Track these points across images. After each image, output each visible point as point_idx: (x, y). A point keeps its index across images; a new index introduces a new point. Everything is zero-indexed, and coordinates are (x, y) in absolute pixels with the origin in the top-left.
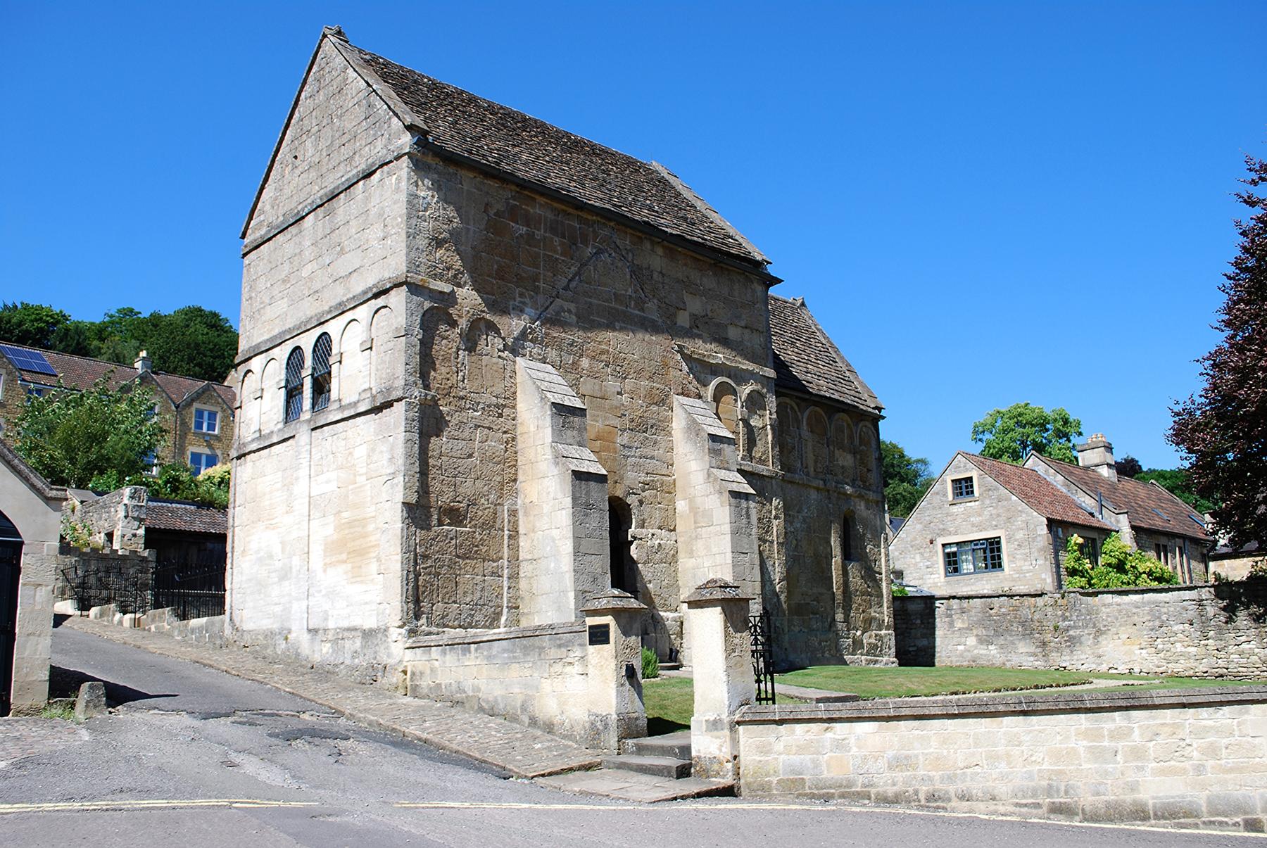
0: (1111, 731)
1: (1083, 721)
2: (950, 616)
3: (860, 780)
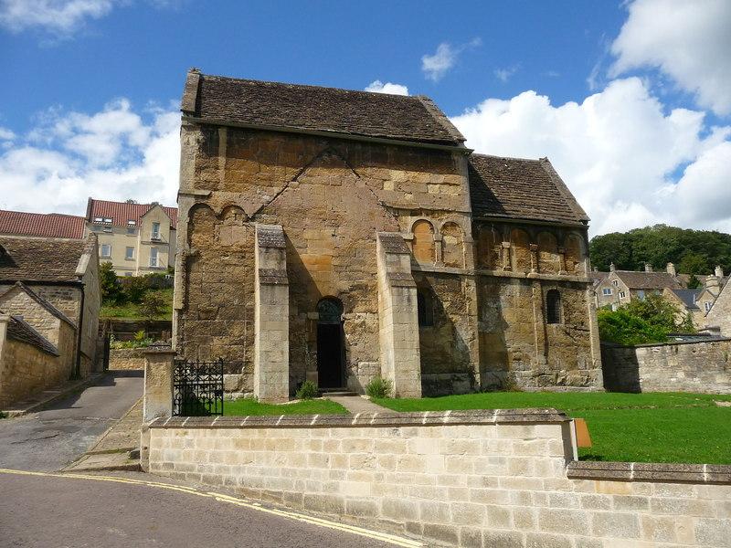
0: (325, 443)
1: (386, 434)
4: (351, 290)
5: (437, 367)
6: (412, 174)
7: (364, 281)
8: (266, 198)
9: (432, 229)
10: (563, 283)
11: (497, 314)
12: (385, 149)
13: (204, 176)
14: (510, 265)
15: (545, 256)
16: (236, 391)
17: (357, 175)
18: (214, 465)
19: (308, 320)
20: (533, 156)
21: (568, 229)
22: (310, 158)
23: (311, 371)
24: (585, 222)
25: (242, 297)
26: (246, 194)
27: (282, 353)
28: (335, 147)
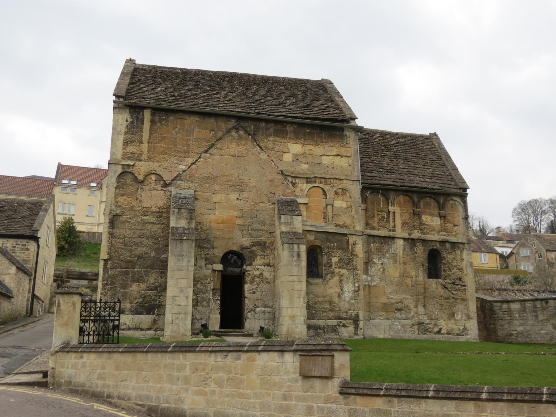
2: (536, 312)
3: (88, 384)
4: (252, 246)
5: (325, 314)
6: (308, 147)
7: (263, 238)
8: (182, 167)
9: (325, 194)
10: (443, 242)
11: (382, 270)
12: (285, 126)
13: (130, 149)
14: (395, 226)
15: (427, 219)
16: (149, 329)
17: (261, 148)
18: (100, 383)
19: (214, 271)
20: (425, 131)
21: (448, 195)
22: (220, 134)
23: (215, 314)
24: (465, 189)
25: (157, 250)
26: (165, 164)
27: (187, 297)
28: (243, 124)
